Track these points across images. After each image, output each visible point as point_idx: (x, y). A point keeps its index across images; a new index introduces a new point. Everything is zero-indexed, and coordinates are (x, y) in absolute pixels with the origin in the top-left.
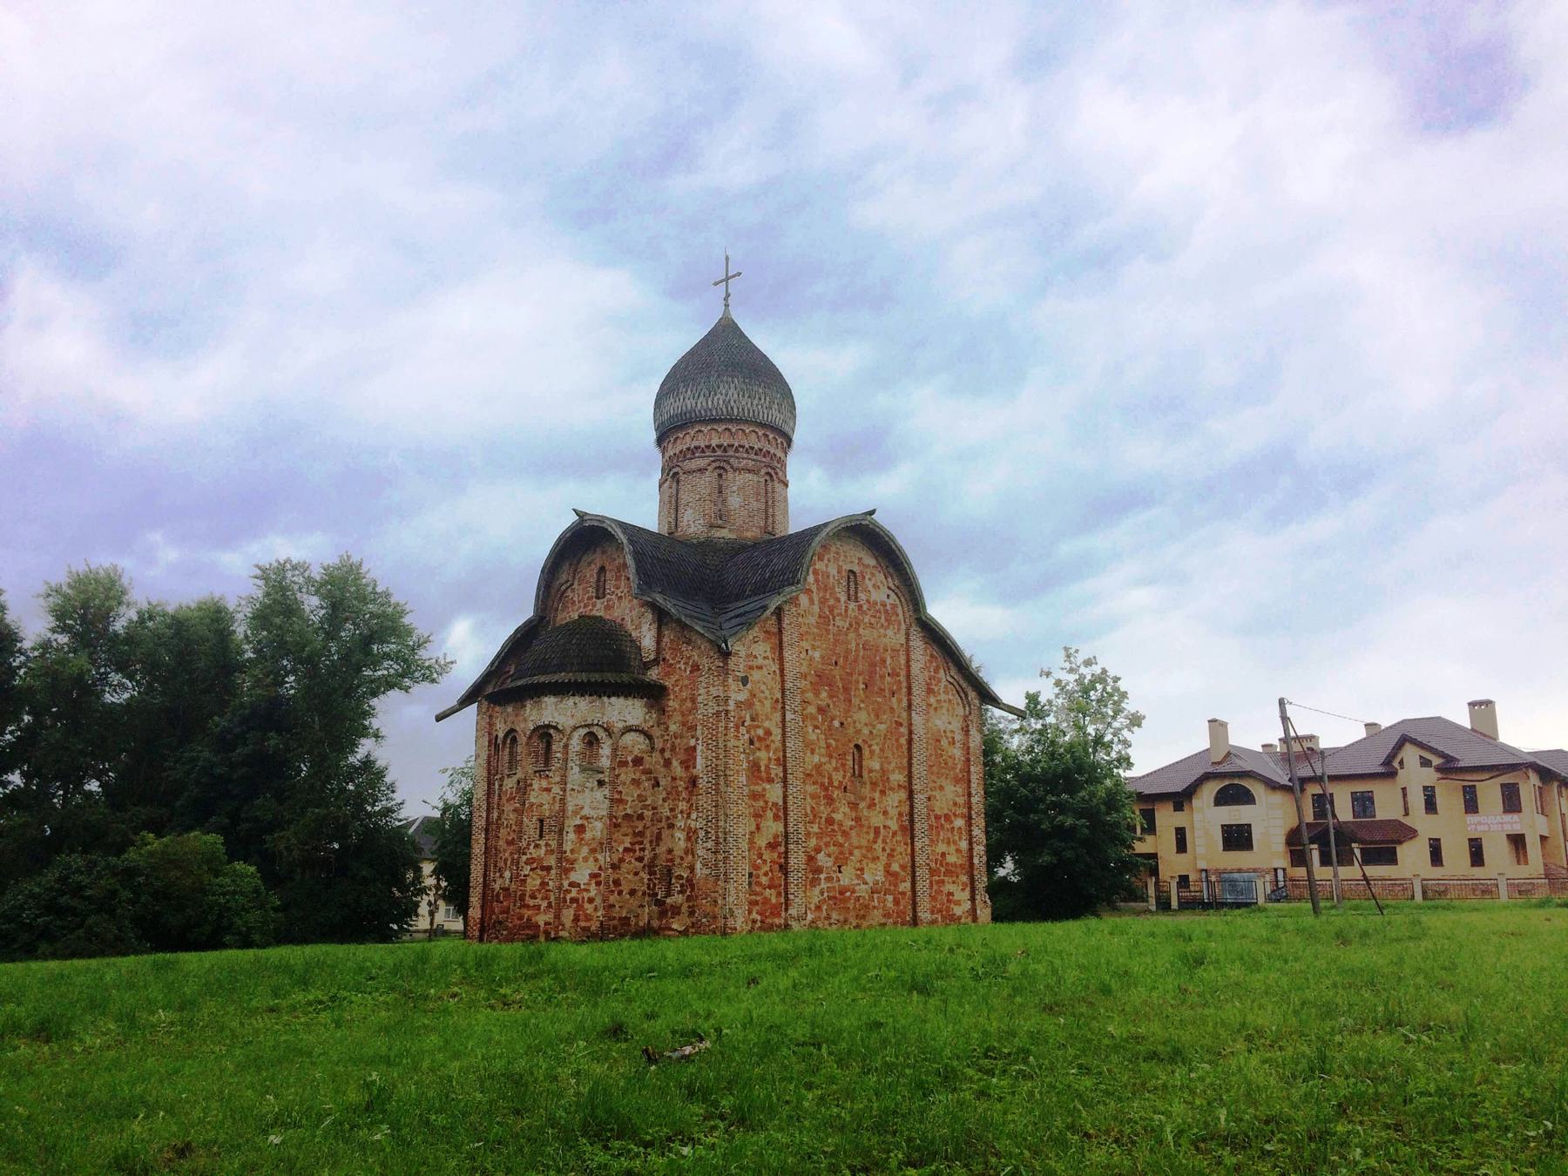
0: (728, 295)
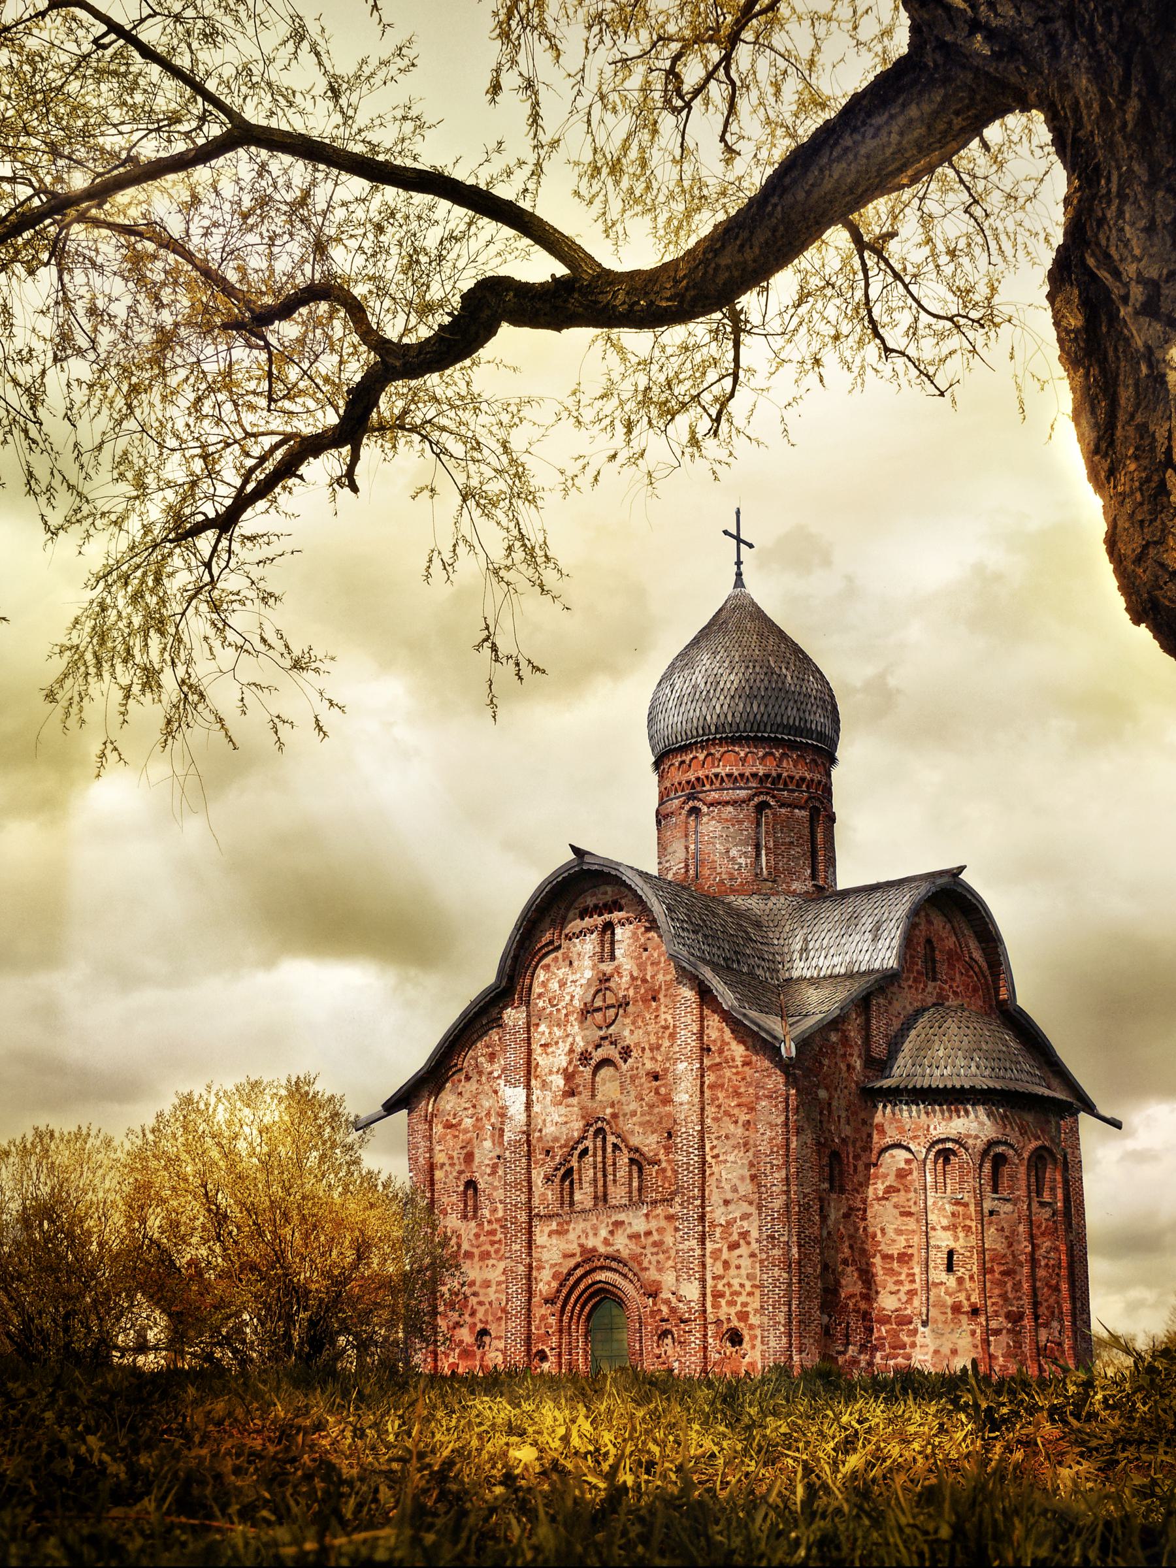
0: (739, 563)
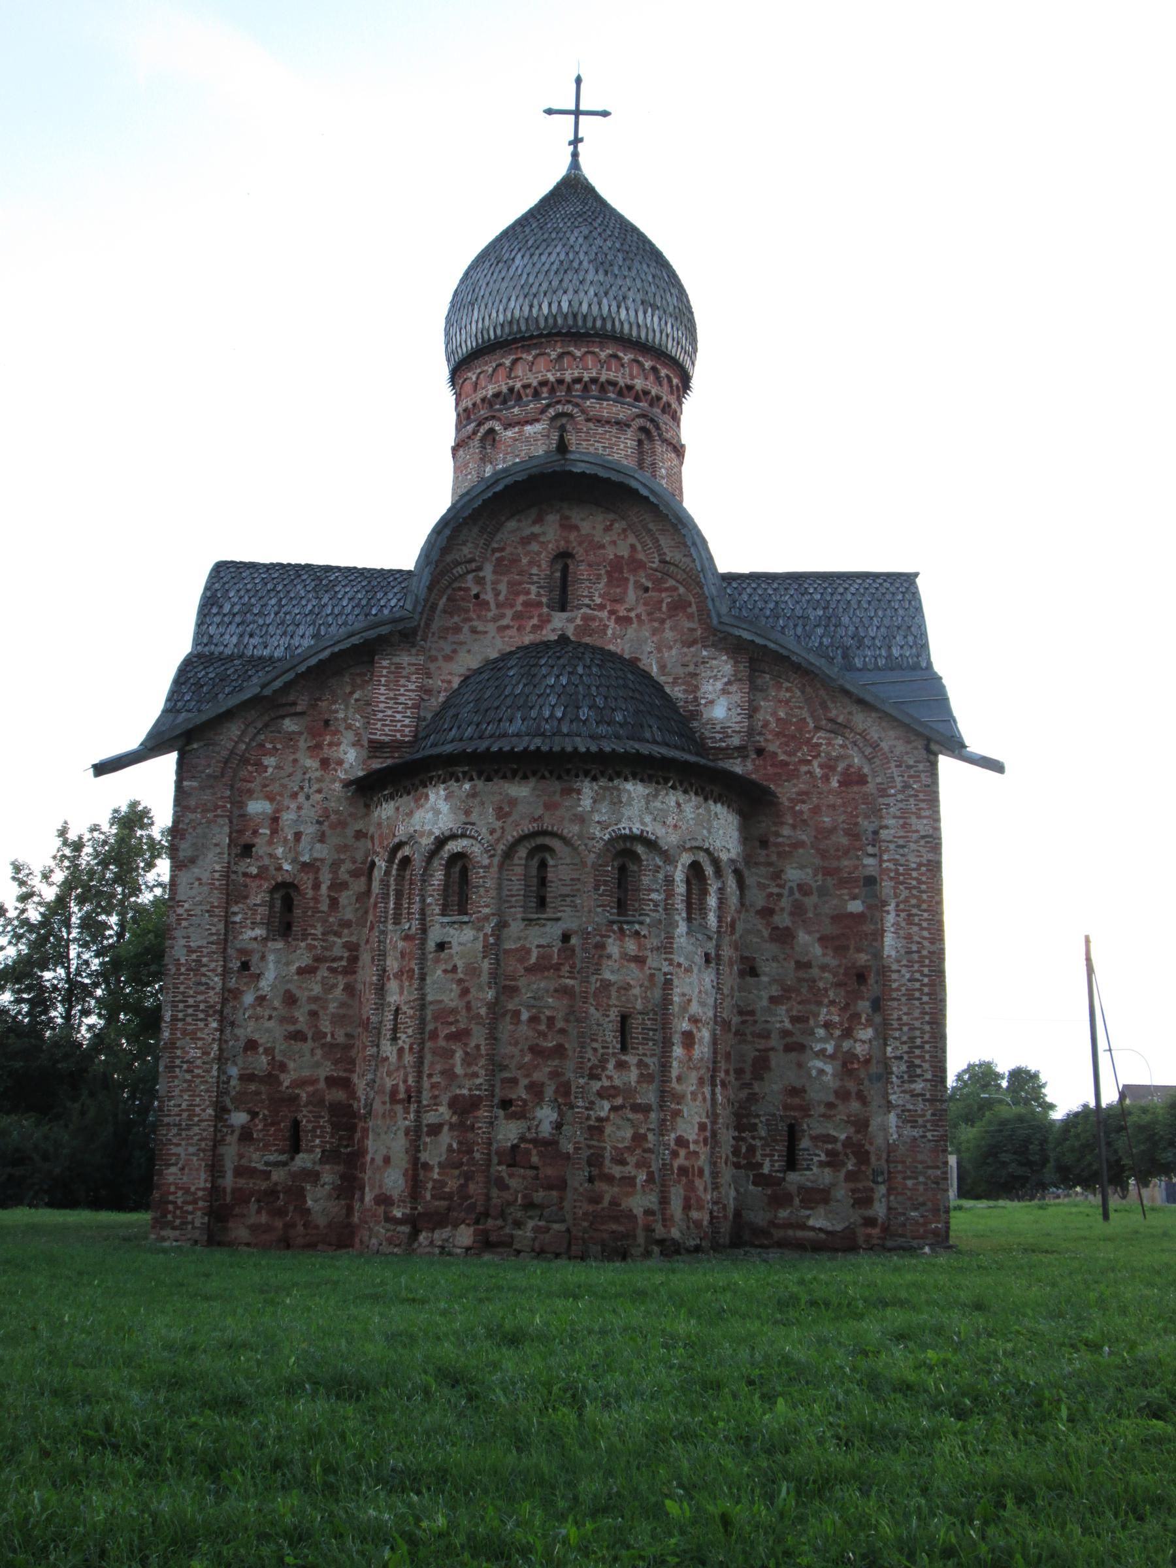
0: (576, 141)
